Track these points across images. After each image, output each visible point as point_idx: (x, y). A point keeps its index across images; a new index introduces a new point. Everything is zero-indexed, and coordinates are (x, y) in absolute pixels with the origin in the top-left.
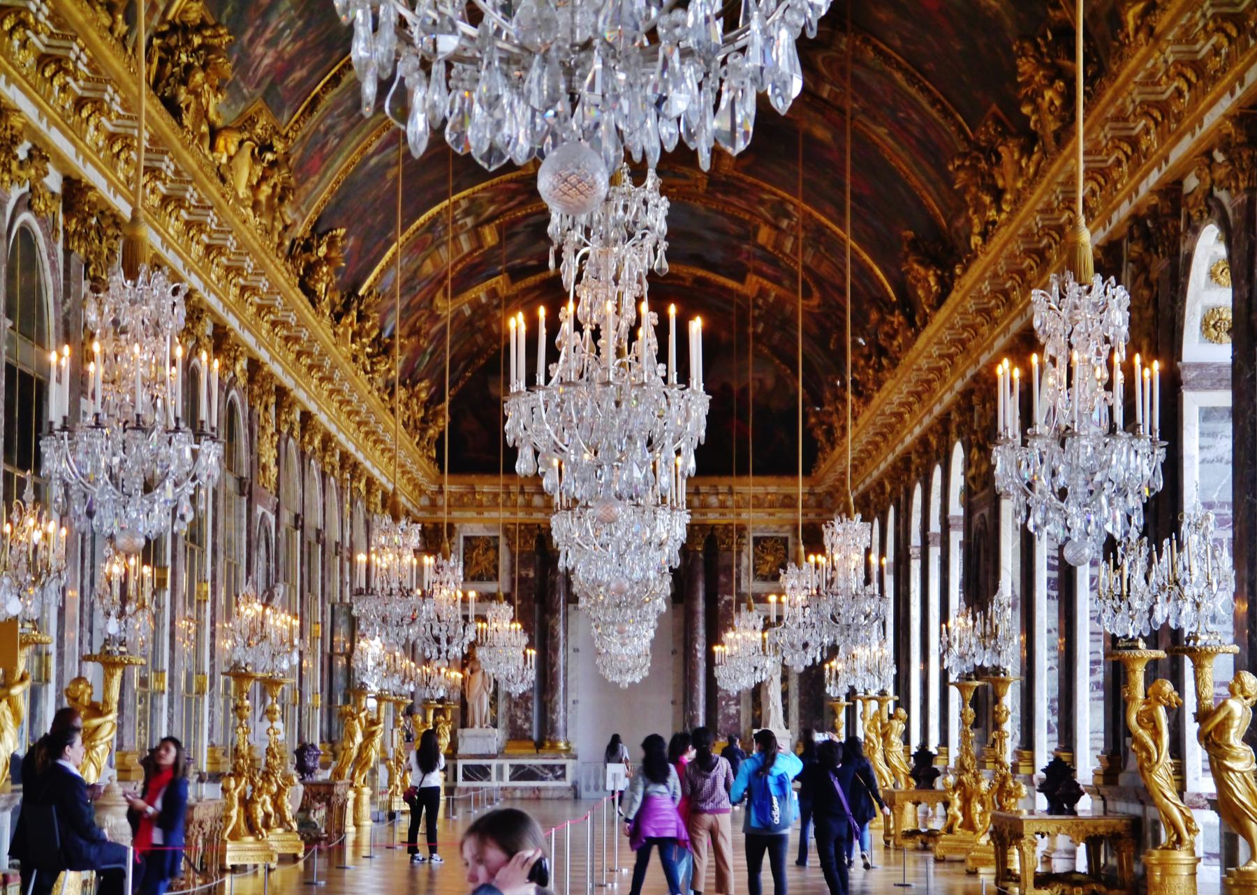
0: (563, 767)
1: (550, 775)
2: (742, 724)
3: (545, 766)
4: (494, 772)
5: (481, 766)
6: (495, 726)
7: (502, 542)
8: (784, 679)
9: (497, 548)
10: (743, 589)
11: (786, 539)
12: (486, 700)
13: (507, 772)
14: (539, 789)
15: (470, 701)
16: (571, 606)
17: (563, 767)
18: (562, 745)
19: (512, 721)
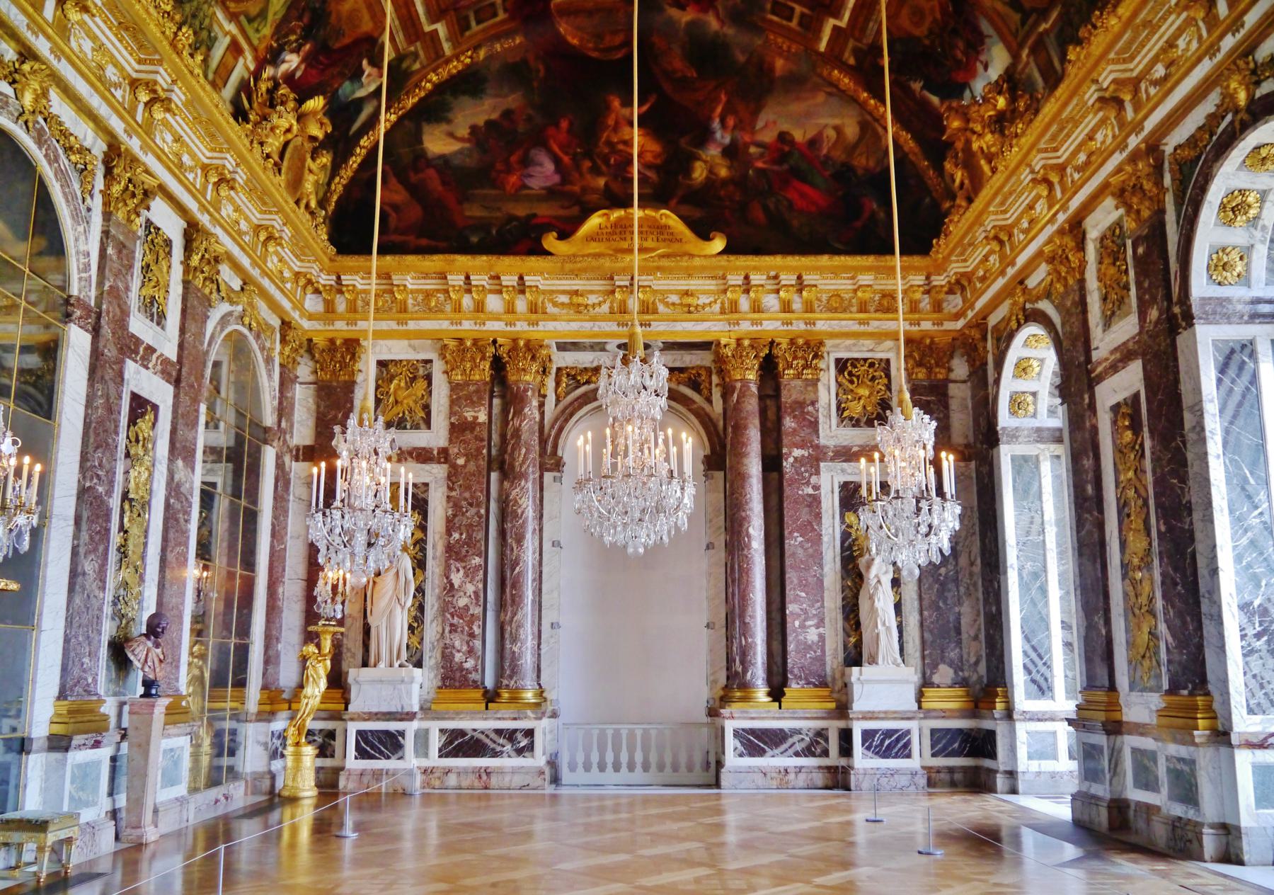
0: (530, 733)
1: (508, 747)
2: (828, 659)
3: (499, 732)
4: (409, 743)
5: (387, 733)
6: (419, 664)
7: (438, 368)
8: (896, 583)
9: (429, 378)
10: (823, 441)
11: (888, 361)
12: (401, 620)
13: (436, 742)
14: (488, 772)
15: (370, 620)
16: (548, 476)
17: (530, 733)
18: (529, 696)
19: (447, 656)
